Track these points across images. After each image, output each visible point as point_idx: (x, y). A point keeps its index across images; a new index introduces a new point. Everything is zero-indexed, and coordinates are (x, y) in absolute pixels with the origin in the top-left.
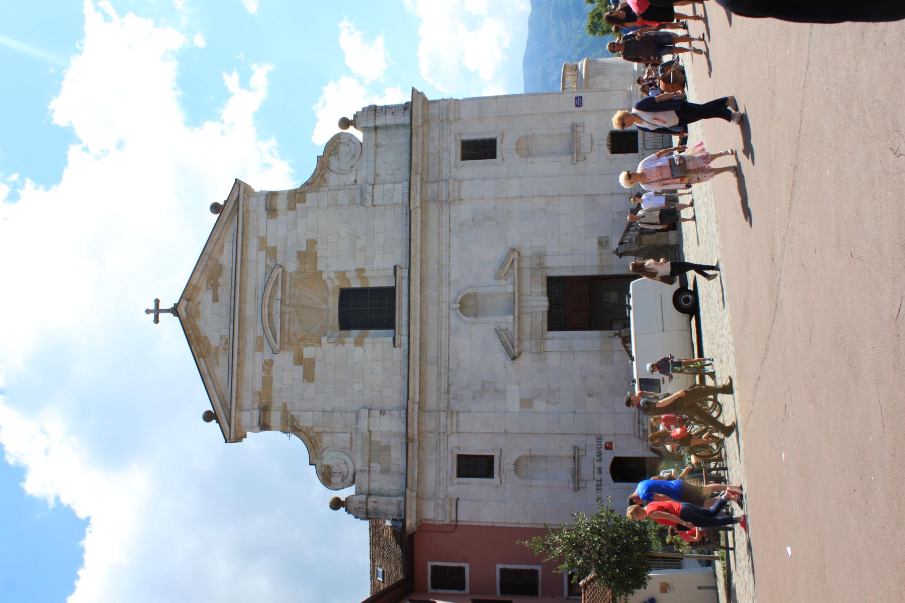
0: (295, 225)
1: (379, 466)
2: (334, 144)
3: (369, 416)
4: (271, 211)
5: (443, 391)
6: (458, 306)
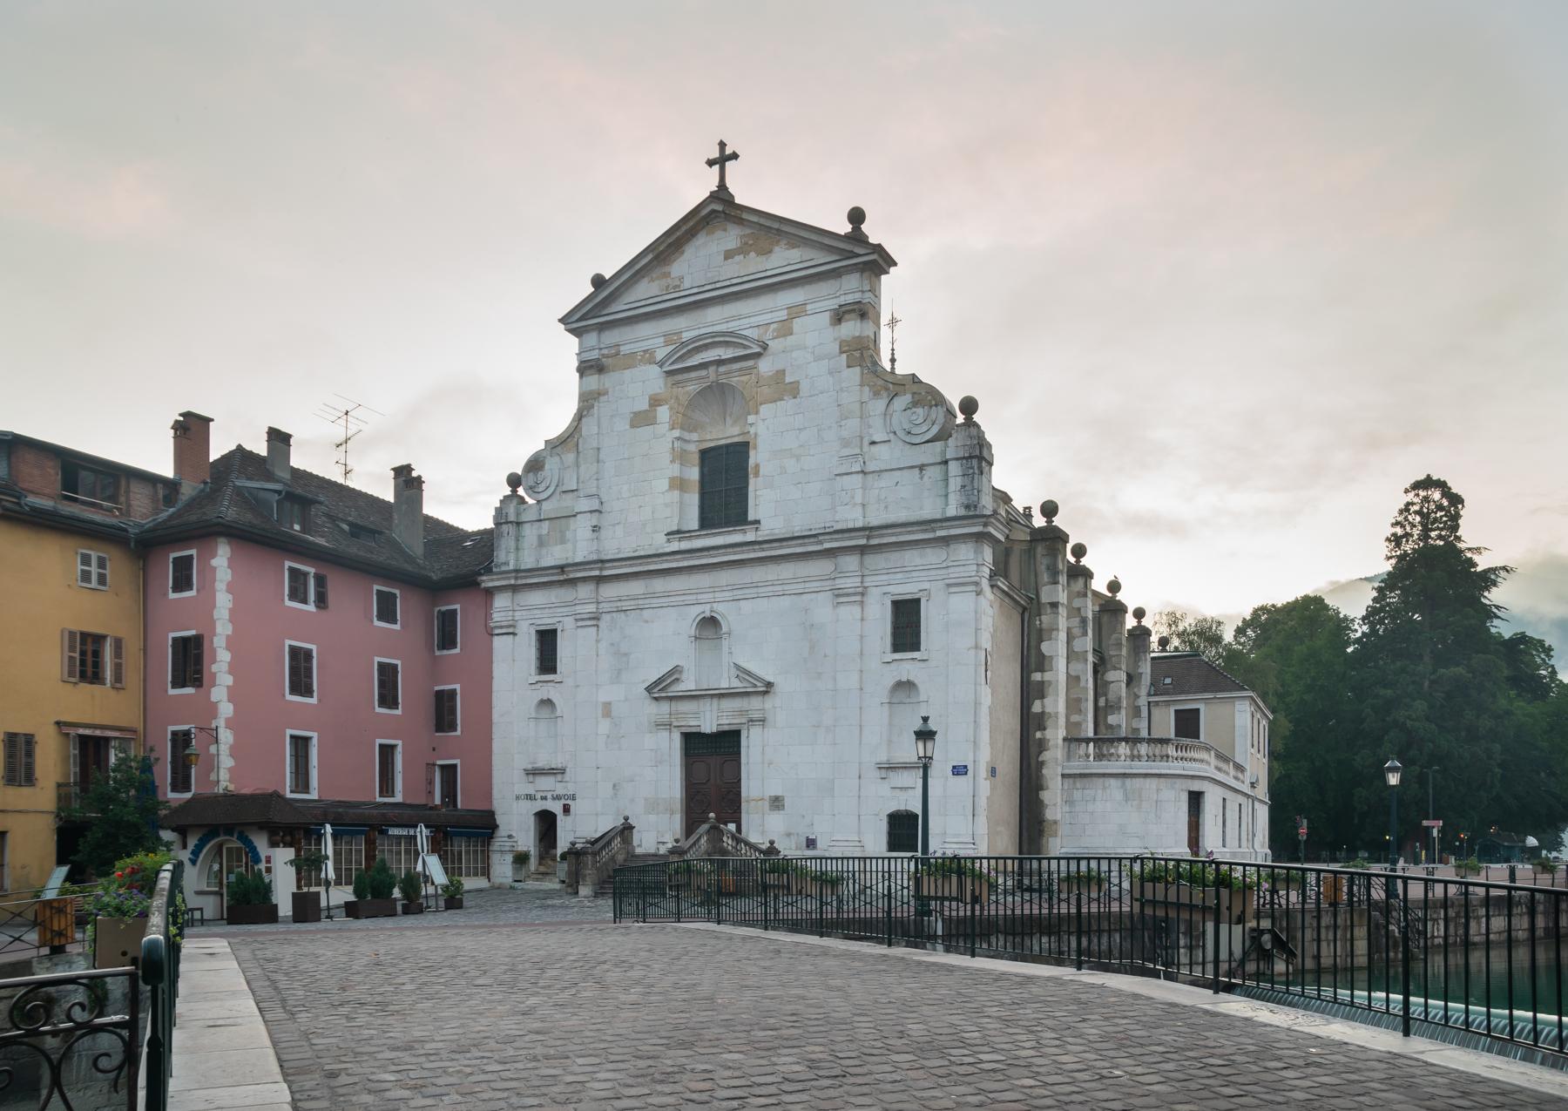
0: (818, 359)
1: (545, 532)
2: (930, 398)
3: (591, 512)
4: (839, 317)
5: (619, 604)
6: (708, 614)
